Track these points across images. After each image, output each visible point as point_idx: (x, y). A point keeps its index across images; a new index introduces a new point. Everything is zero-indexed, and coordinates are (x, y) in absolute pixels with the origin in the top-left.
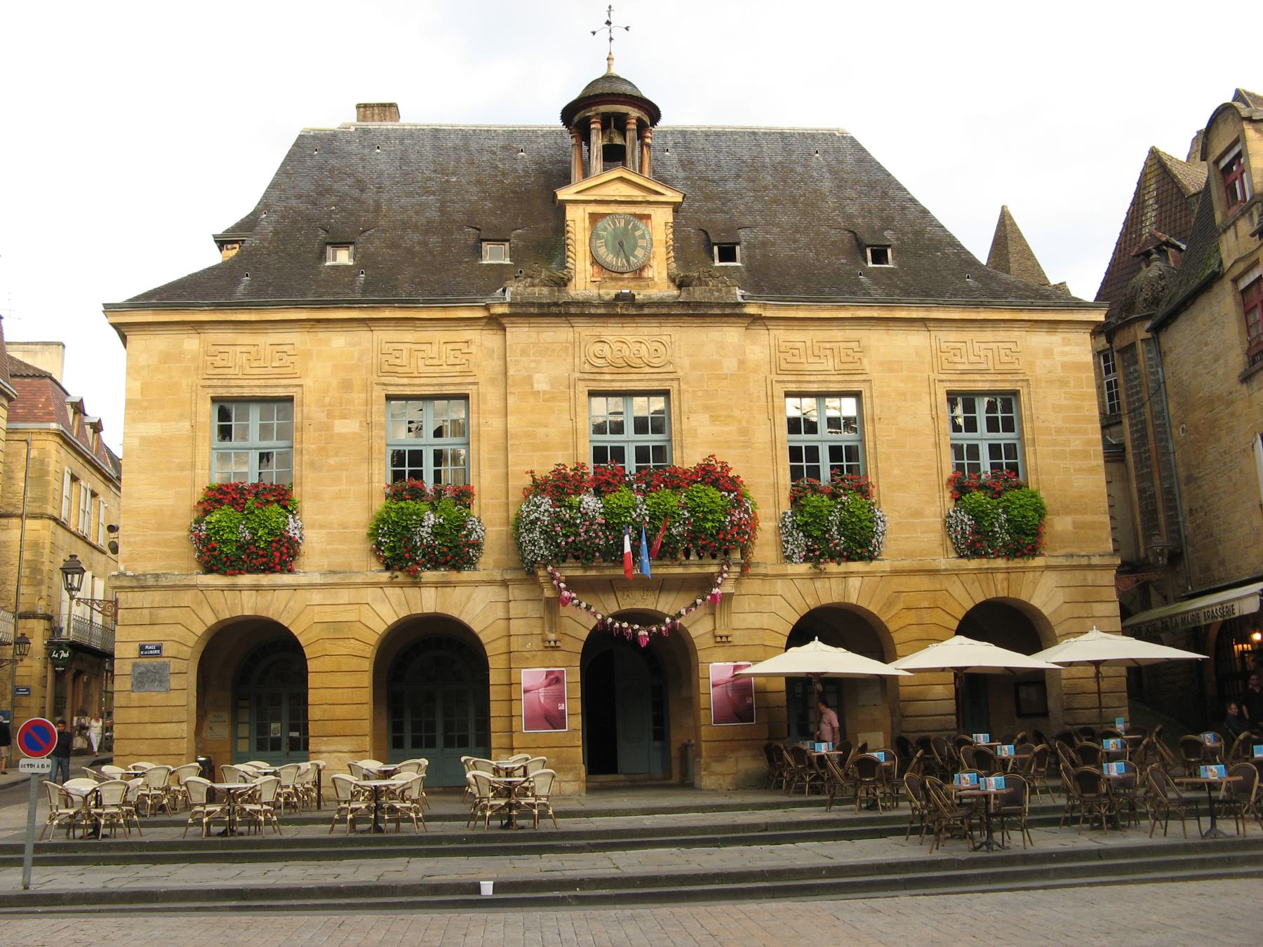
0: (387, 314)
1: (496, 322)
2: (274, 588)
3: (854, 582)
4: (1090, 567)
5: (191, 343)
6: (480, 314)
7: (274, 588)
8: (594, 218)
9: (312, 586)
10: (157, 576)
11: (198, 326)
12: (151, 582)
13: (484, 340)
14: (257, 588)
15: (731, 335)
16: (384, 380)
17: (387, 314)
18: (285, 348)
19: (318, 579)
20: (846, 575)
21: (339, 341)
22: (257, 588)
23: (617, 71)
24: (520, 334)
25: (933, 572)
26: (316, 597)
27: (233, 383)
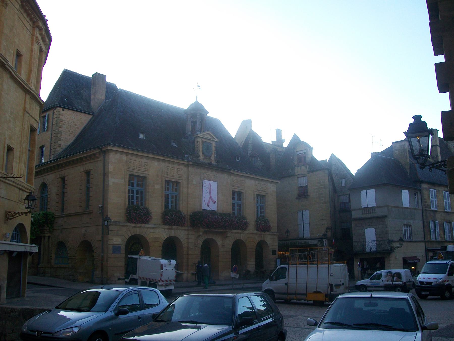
0: (168, 159)
1: (188, 166)
2: (144, 227)
3: (242, 235)
4: (275, 235)
5: (124, 158)
6: (186, 163)
7: (144, 227)
8: (203, 142)
9: (152, 228)
10: (119, 222)
11: (127, 154)
12: (118, 224)
13: (184, 169)
14: (140, 227)
15: (225, 176)
16: (165, 176)
17: (168, 159)
18: (146, 164)
19: (153, 226)
20: (241, 233)
21: (156, 164)
22: (140, 227)
23: (200, 101)
24: (191, 169)
25: (253, 234)
26: (152, 230)
27: (134, 171)
